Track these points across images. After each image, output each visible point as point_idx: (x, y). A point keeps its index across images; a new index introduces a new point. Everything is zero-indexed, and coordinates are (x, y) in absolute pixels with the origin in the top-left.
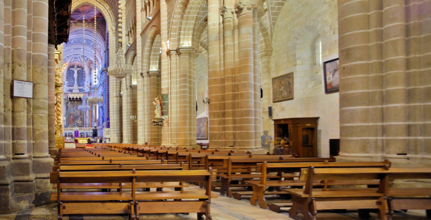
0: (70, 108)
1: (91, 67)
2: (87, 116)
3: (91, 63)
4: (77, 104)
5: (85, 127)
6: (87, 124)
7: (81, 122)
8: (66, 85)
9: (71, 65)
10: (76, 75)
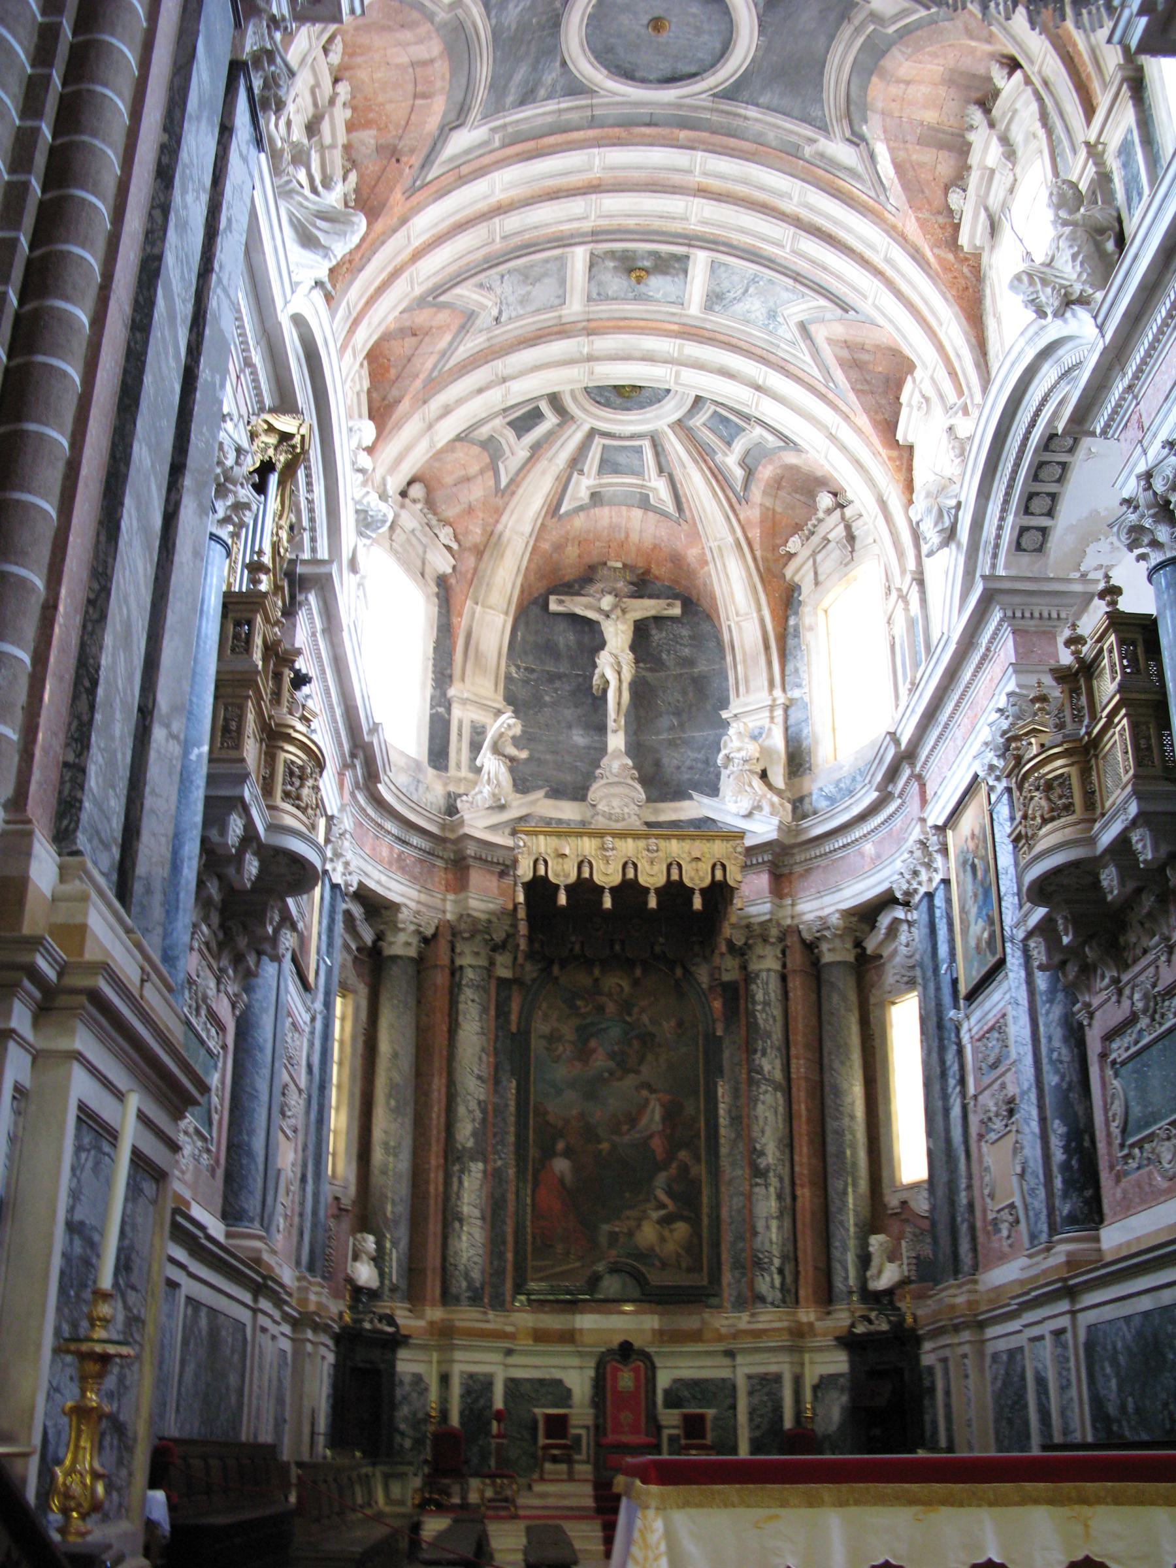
0: (537, 1045)
1: (789, 572)
2: (762, 1154)
3: (797, 528)
4: (626, 1007)
5: (741, 1304)
6: (759, 1264)
7: (681, 1229)
8: (496, 750)
9: (559, 547)
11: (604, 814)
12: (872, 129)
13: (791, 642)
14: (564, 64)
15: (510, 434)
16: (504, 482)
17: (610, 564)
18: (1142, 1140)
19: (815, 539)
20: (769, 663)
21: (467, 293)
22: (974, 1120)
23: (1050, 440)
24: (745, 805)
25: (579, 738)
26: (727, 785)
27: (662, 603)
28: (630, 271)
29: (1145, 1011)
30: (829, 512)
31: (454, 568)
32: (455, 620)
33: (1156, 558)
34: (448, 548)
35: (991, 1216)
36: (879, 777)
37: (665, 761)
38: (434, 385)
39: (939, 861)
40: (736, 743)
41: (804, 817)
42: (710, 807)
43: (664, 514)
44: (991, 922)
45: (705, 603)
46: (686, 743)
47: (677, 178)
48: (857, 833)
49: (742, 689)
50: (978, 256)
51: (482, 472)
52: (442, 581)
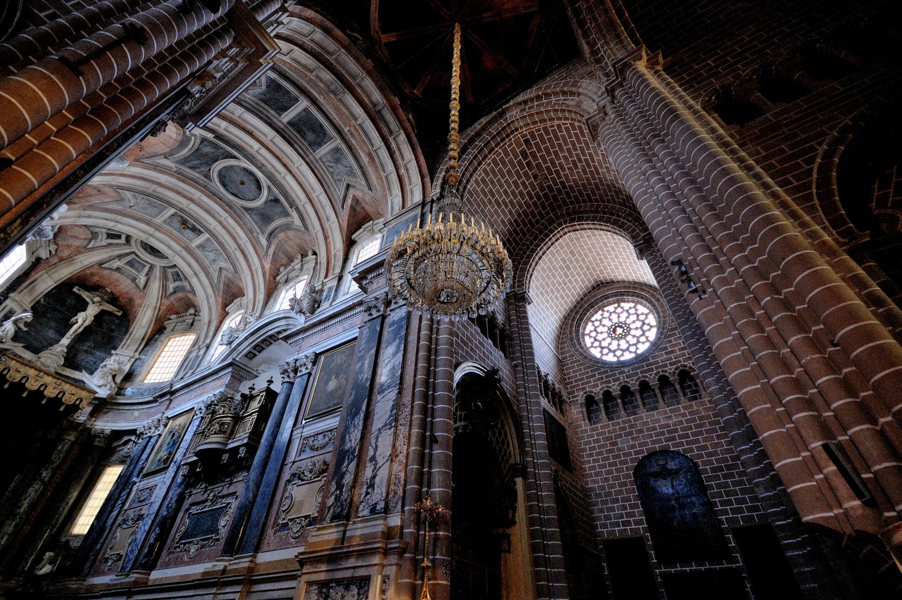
1: (166, 323)
3: (178, 313)
8: (15, 322)
9: (92, 275)
10: (83, 319)
11: (41, 362)
12: (275, 242)
13: (152, 342)
14: (210, 170)
15: (105, 236)
16: (90, 246)
17: (107, 289)
18: (186, 543)
19: (181, 319)
20: (140, 344)
21: (128, 194)
22: (120, 518)
23: (271, 336)
24: (101, 382)
25: (51, 334)
26: (98, 373)
27: (116, 309)
28: (183, 224)
29: (211, 501)
30: (191, 315)
31: (47, 258)
32: (33, 273)
33: (287, 379)
34: (50, 252)
35: (106, 556)
36: (157, 395)
37: (79, 356)
38: (92, 207)
39: (162, 427)
40: (112, 362)
41: (120, 395)
42: (87, 379)
43: (138, 286)
44: (170, 453)
45: (131, 317)
46: (91, 354)
47: (216, 215)
48: (136, 407)
49: (125, 347)
50: (278, 284)
51: (85, 239)
52: (38, 260)
